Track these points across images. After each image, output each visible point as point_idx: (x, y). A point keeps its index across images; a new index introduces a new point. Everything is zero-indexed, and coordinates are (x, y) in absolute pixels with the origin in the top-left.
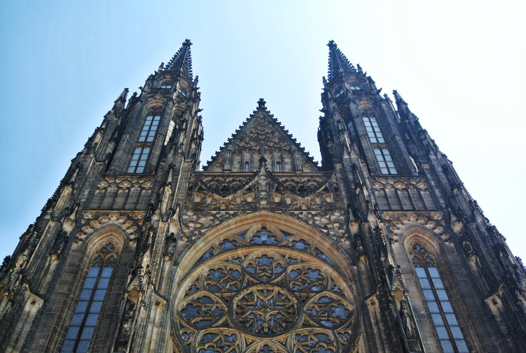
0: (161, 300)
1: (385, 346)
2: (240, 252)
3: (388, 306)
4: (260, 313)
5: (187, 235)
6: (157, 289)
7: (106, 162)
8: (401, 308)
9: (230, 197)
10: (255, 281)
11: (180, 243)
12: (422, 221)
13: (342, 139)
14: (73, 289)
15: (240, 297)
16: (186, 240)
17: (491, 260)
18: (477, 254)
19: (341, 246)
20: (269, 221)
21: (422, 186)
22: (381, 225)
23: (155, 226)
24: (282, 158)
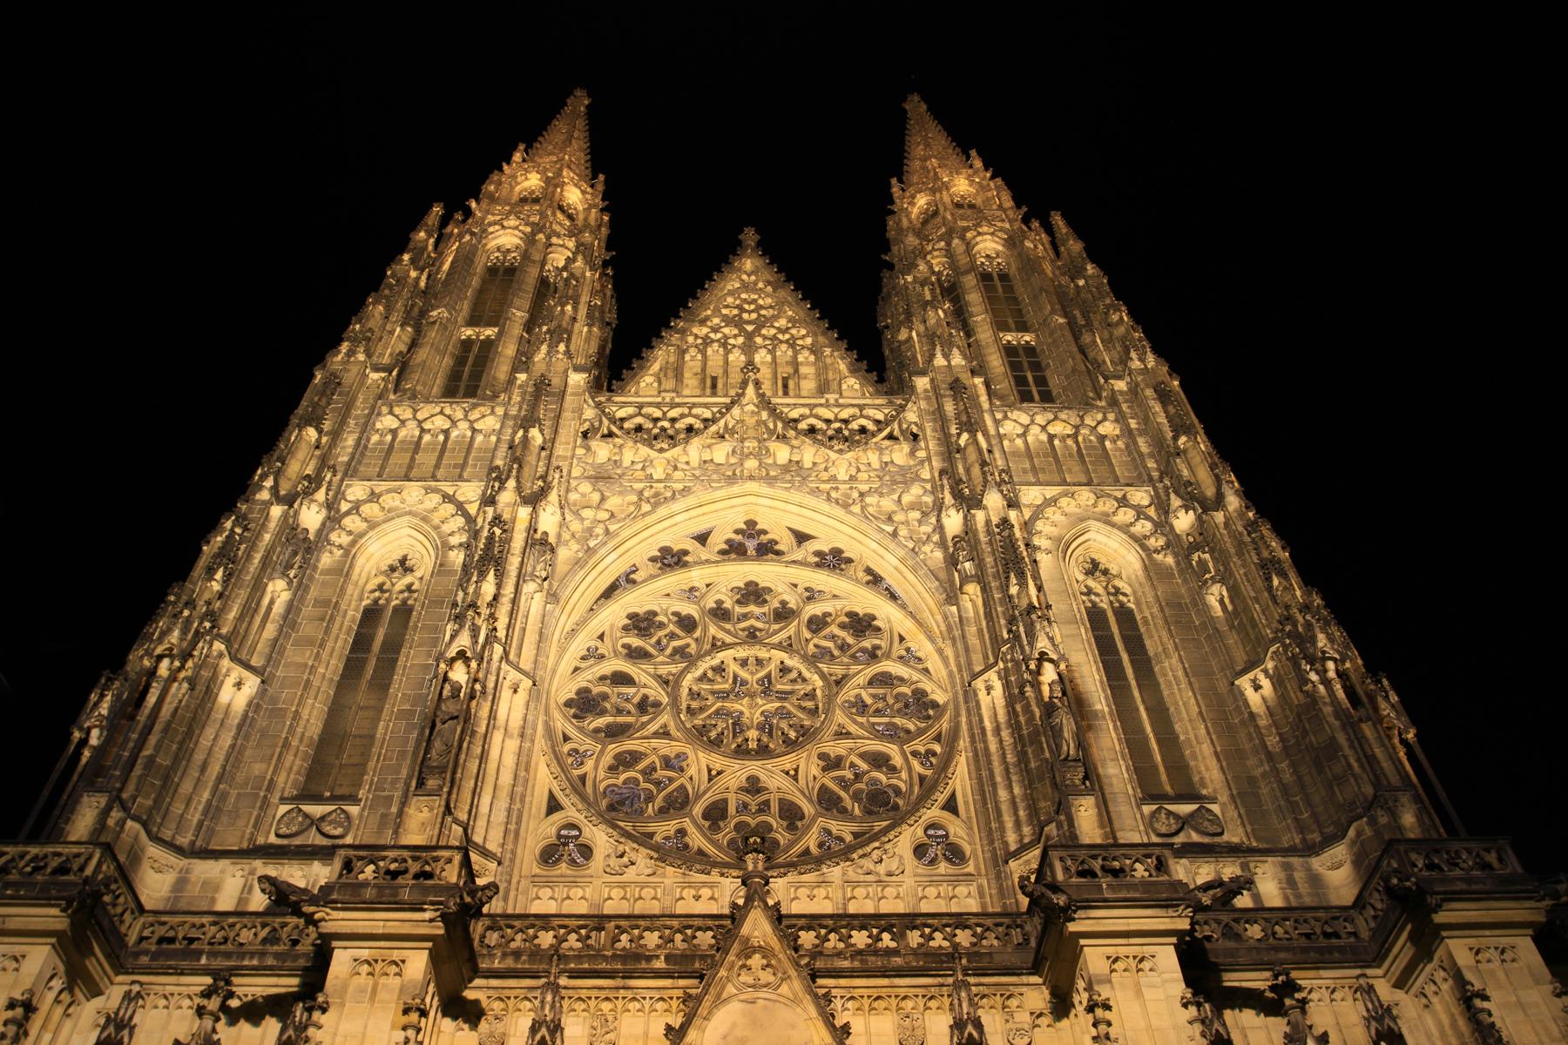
1: (1014, 778)
2: (695, 576)
4: (737, 706)
6: (512, 657)
9: (678, 450)
11: (564, 554)
12: (1108, 506)
14: (324, 656)
15: (699, 673)
17: (1253, 594)
18: (1222, 581)
22: (1013, 515)
23: (506, 516)
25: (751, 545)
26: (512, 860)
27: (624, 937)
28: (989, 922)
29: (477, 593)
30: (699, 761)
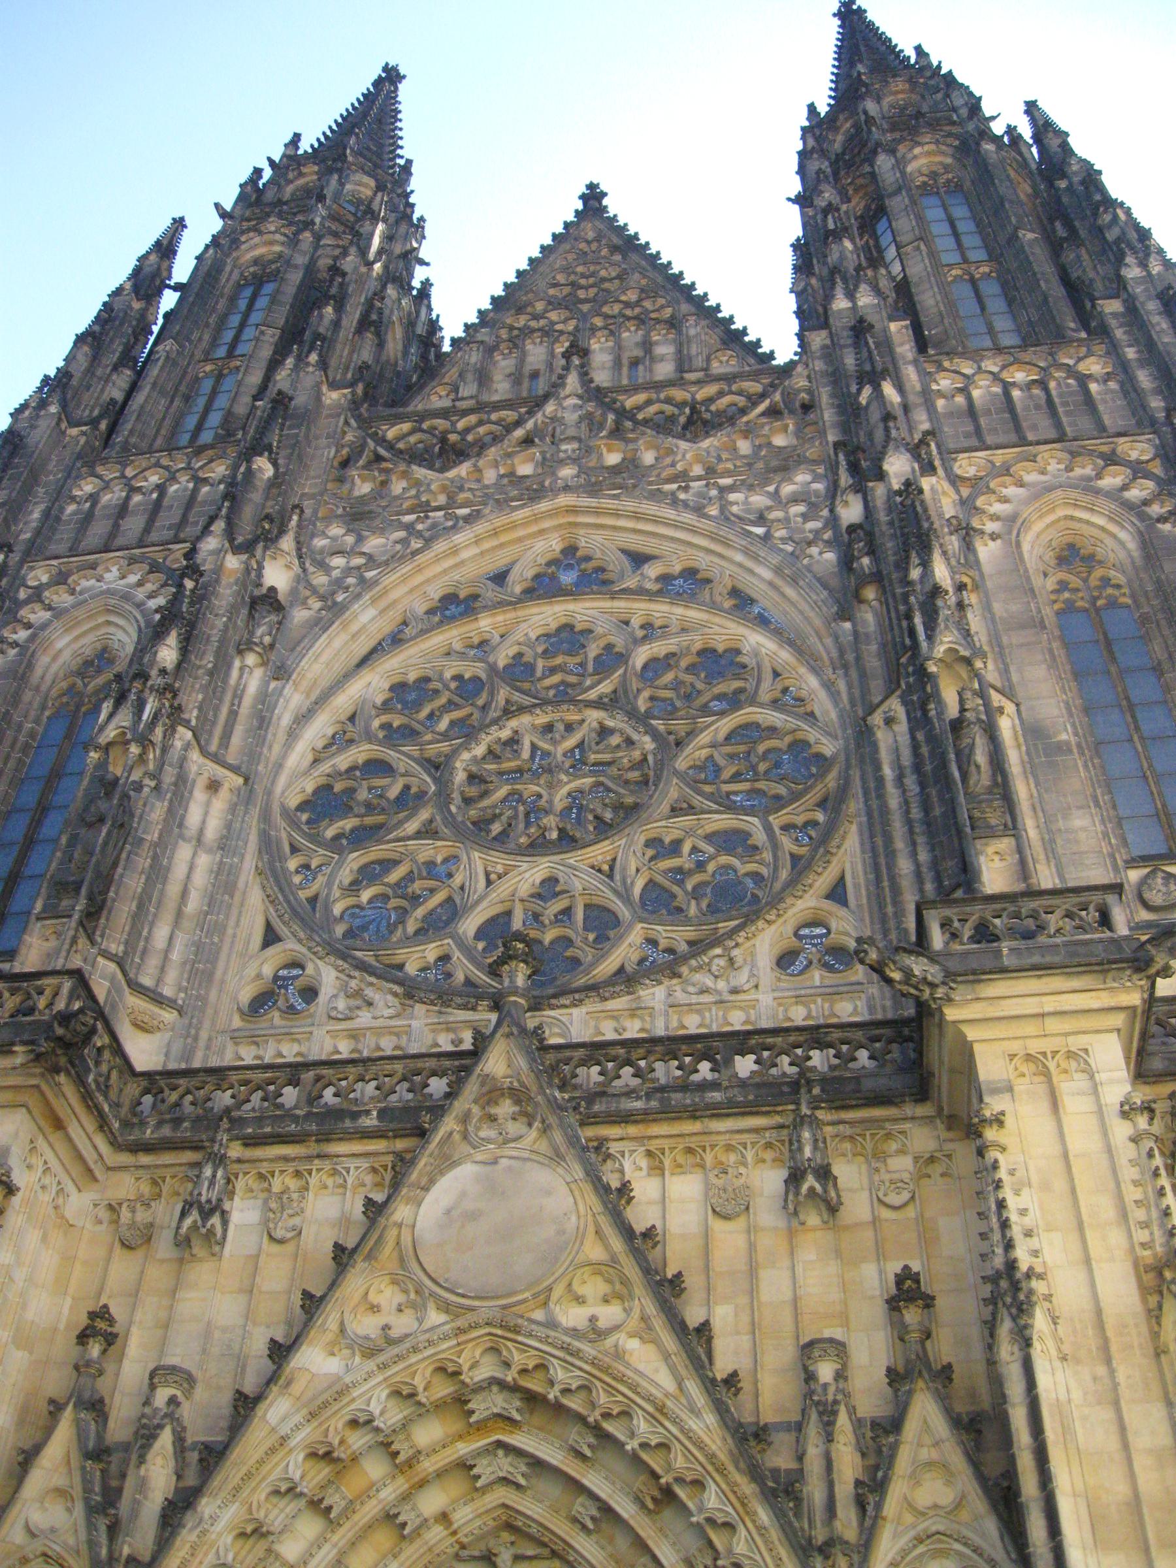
0: (221, 772)
1: (920, 840)
2: (485, 624)
3: (925, 712)
5: (322, 591)
6: (213, 748)
7: (103, 425)
8: (963, 710)
9: (463, 470)
10: (527, 701)
11: (299, 615)
13: (833, 258)
15: (480, 750)
16: (318, 605)
19: (809, 568)
20: (588, 525)
21: (1094, 366)
22: (926, 483)
24: (647, 345)
25: (568, 578)
26: (203, 1011)
27: (328, 1093)
28: (859, 1035)
29: (153, 662)
30: (476, 862)
